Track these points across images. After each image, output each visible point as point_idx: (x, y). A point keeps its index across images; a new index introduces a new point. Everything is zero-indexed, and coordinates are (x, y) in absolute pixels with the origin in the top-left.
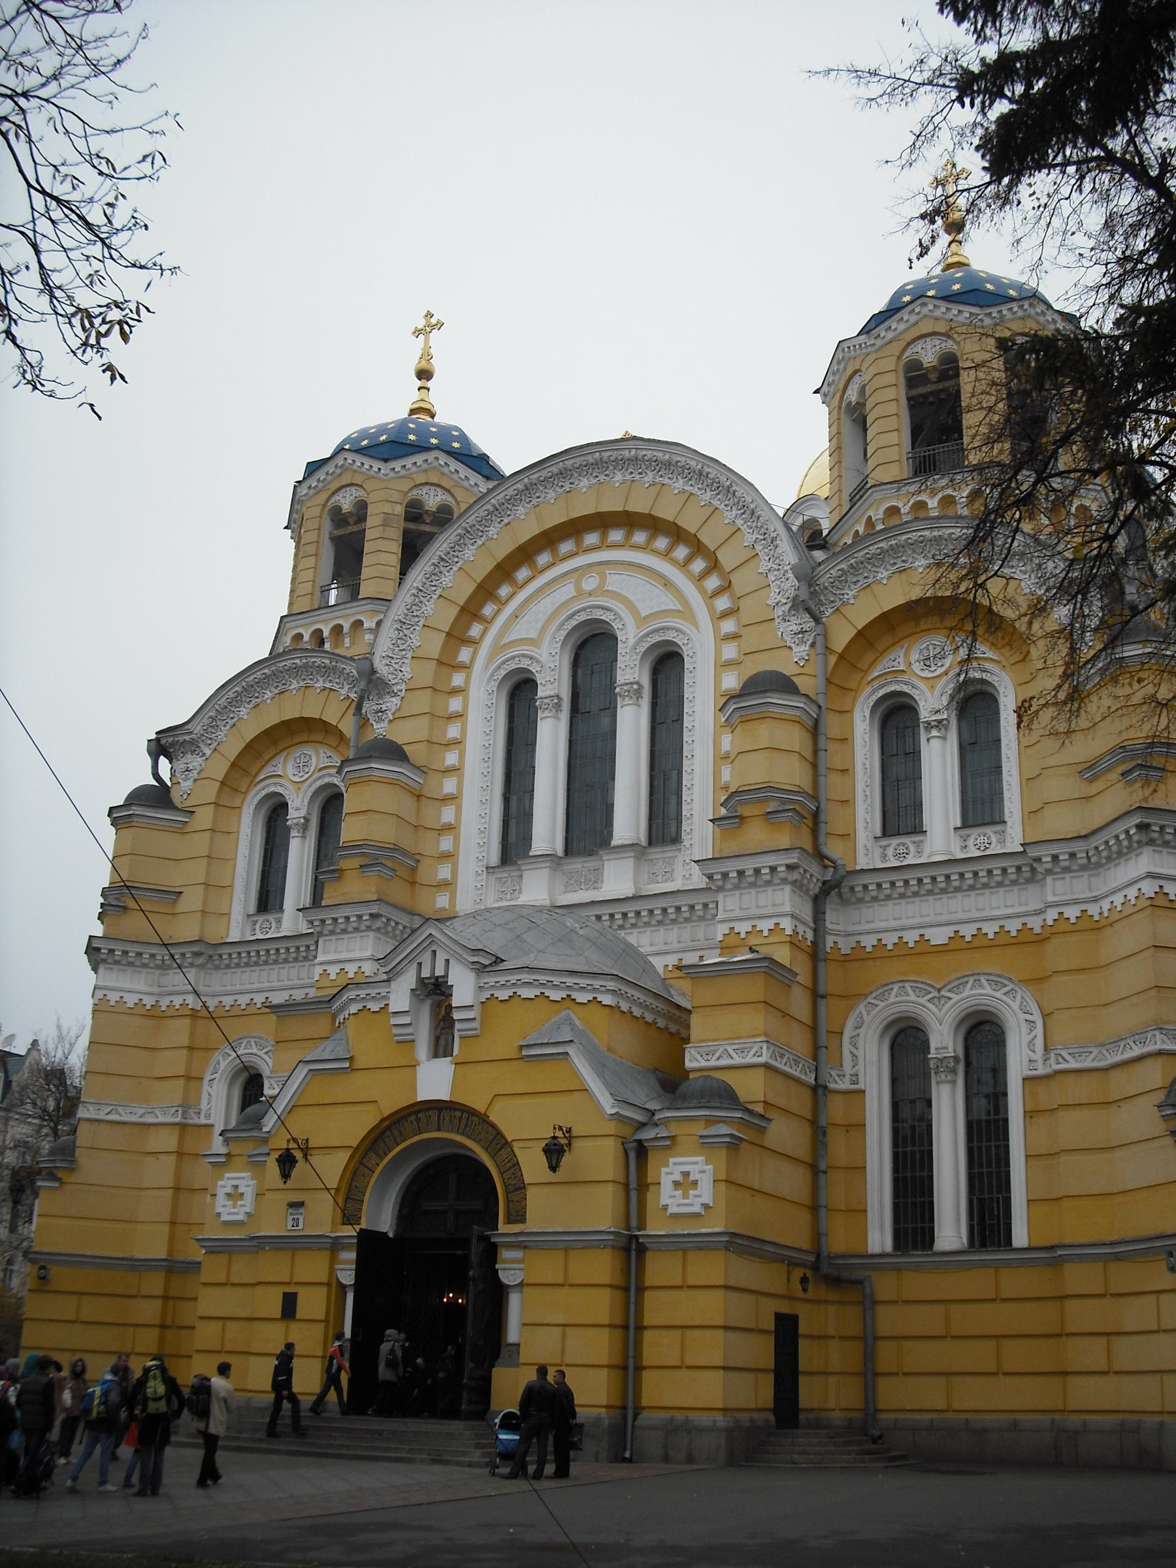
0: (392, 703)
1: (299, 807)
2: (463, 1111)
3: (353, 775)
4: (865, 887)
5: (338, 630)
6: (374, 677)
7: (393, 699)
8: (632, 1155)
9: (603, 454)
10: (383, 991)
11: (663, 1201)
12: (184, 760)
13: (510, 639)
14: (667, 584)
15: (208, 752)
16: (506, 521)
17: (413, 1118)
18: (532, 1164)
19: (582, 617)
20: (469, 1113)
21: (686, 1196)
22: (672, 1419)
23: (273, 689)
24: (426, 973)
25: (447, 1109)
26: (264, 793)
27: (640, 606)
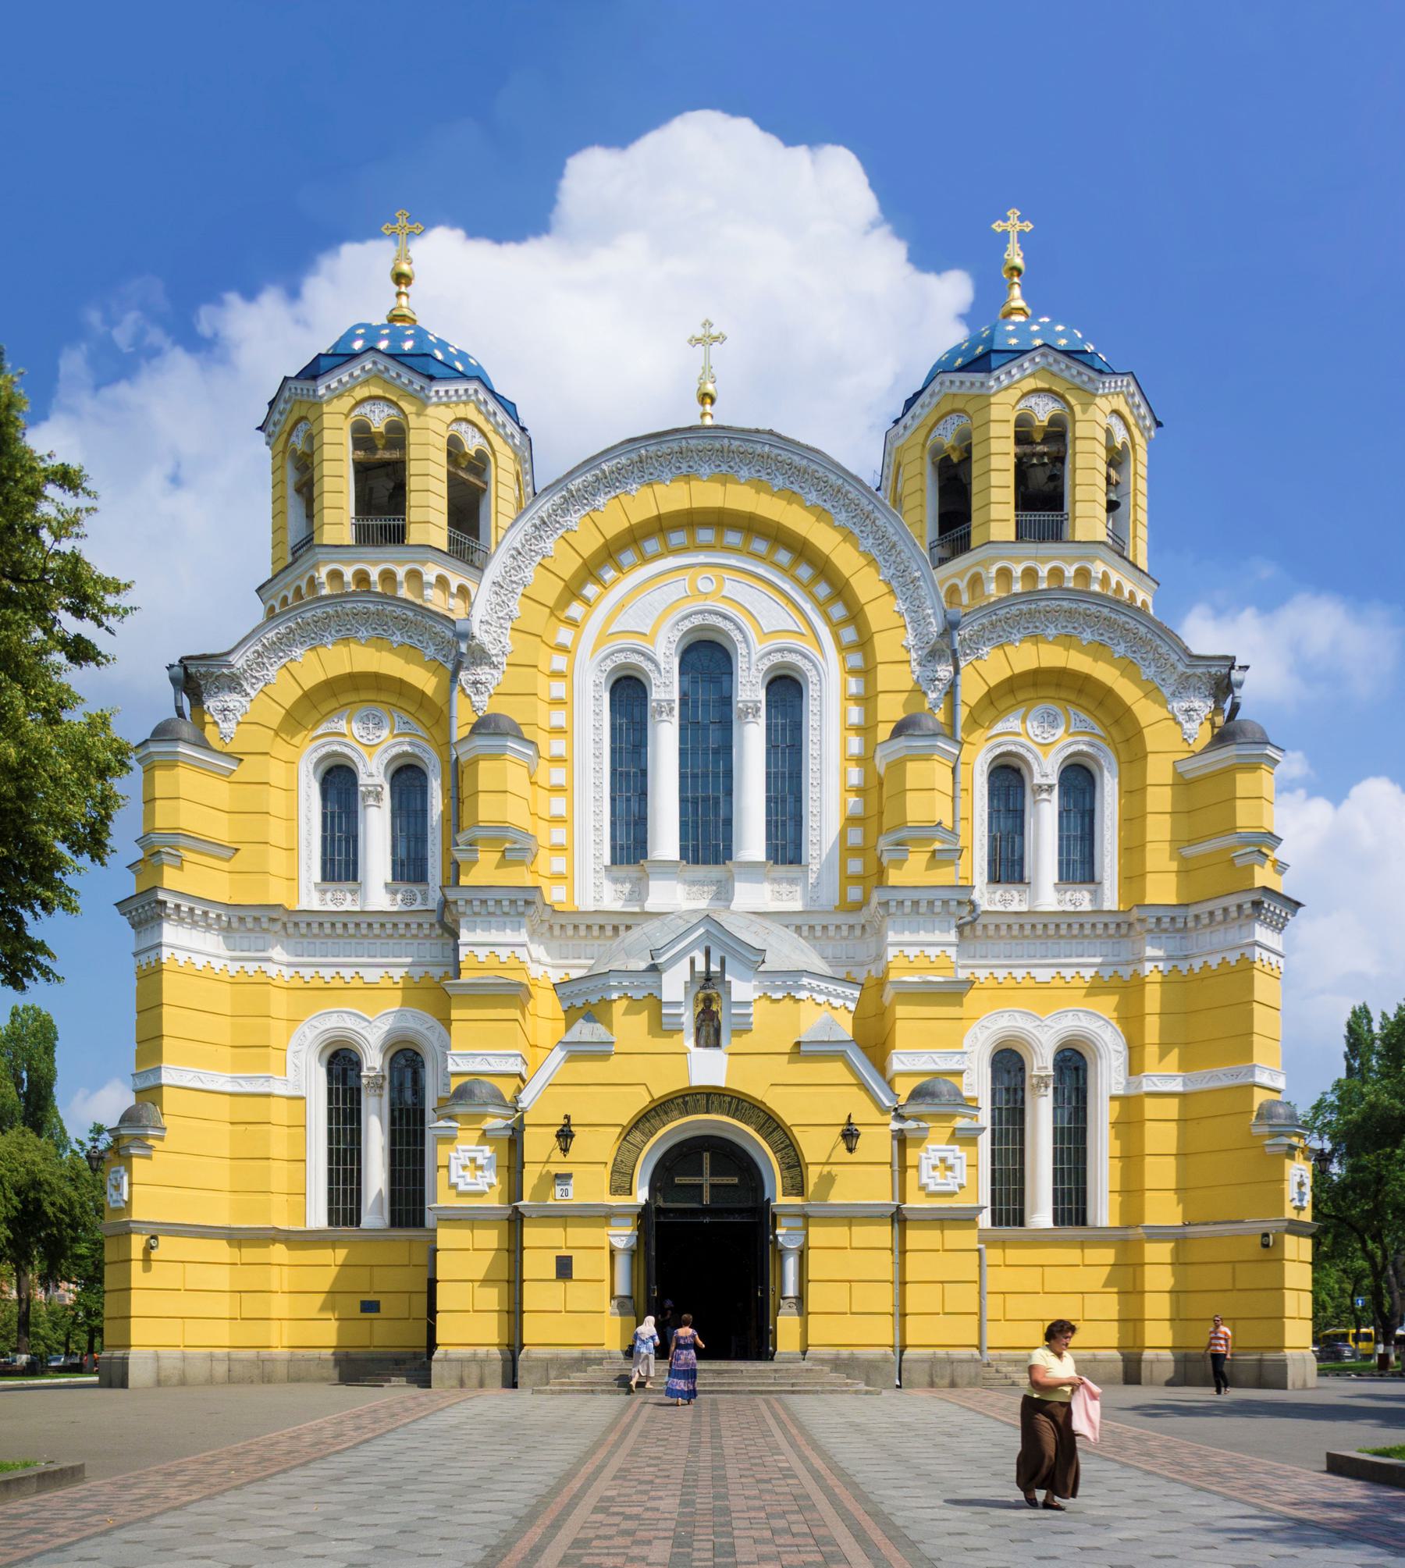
2: (732, 1097)
5: (388, 577)
6: (473, 643)
8: (895, 1143)
15: (253, 693)
17: (681, 1100)
18: (816, 1146)
19: (697, 620)
20: (739, 1099)
22: (935, 1353)
23: (333, 632)
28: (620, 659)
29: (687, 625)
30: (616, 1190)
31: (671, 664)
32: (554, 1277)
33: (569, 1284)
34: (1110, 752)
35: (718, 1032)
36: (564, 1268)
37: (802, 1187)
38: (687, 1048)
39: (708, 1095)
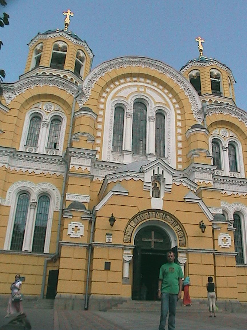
0: (85, 100)
1: (47, 118)
3: (83, 114)
7: (86, 99)
9: (151, 62)
10: (140, 175)
12: (8, 93)
13: (118, 95)
14: (162, 97)
15: (17, 94)
16: (120, 67)
17: (147, 213)
23: (43, 84)
24: (156, 173)
25: (158, 212)
26: (34, 112)
27: (156, 100)
29: (137, 97)
32: (104, 269)
33: (109, 272)
34: (240, 143)
35: (159, 193)
36: (108, 266)
37: (185, 244)
38: (151, 197)
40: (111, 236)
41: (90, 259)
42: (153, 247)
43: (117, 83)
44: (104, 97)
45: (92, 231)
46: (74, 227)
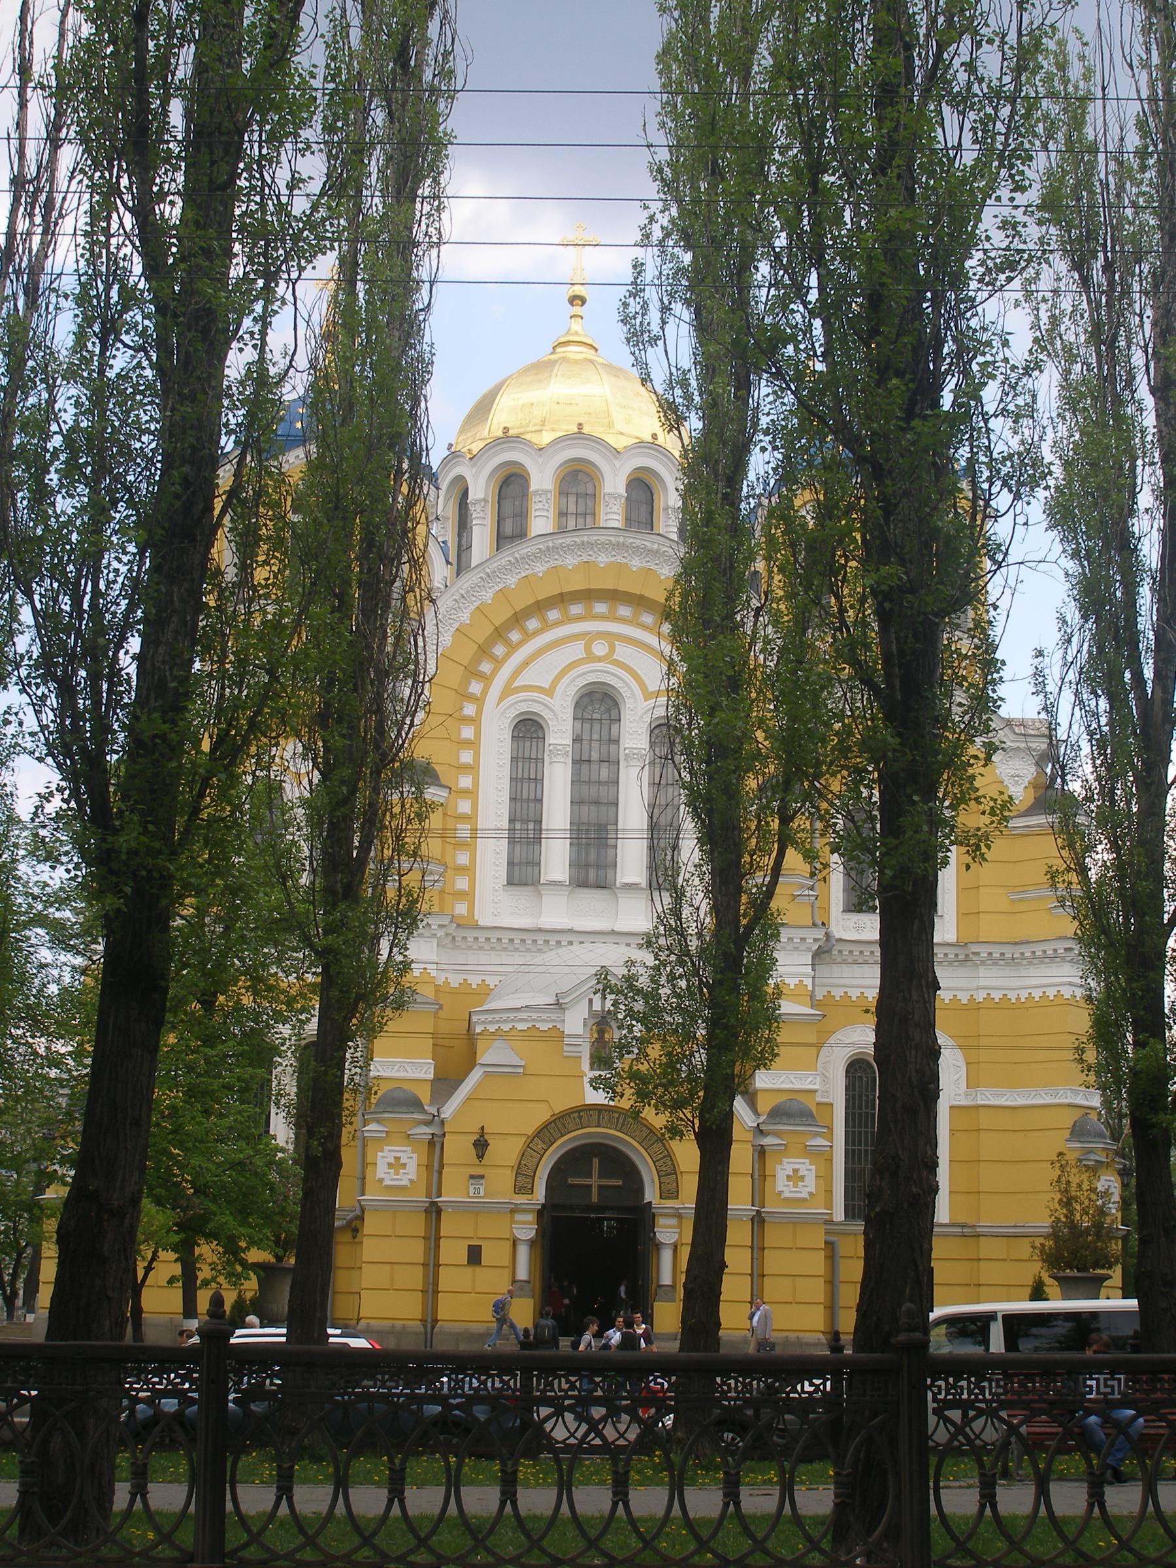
4: (840, 951)
8: (756, 1156)
11: (780, 1188)
21: (796, 1186)
24: (597, 1006)
28: (524, 707)
30: (519, 1190)
31: (569, 714)
33: (478, 1269)
36: (475, 1255)
39: (600, 1111)
40: (483, 1181)
41: (433, 1239)
42: (595, 1198)
43: (515, 636)
44: (472, 698)
45: (436, 1167)
46: (392, 1161)
